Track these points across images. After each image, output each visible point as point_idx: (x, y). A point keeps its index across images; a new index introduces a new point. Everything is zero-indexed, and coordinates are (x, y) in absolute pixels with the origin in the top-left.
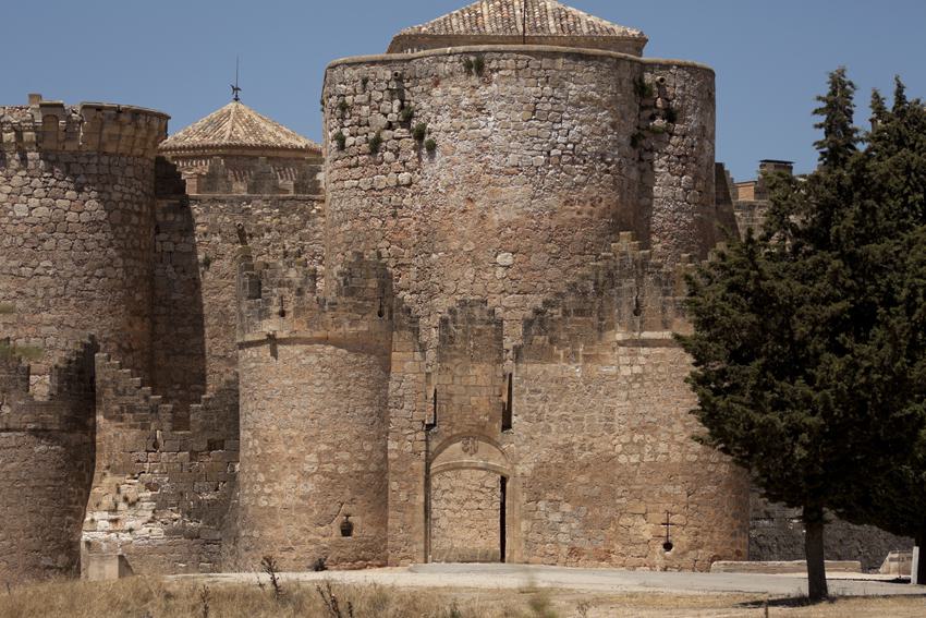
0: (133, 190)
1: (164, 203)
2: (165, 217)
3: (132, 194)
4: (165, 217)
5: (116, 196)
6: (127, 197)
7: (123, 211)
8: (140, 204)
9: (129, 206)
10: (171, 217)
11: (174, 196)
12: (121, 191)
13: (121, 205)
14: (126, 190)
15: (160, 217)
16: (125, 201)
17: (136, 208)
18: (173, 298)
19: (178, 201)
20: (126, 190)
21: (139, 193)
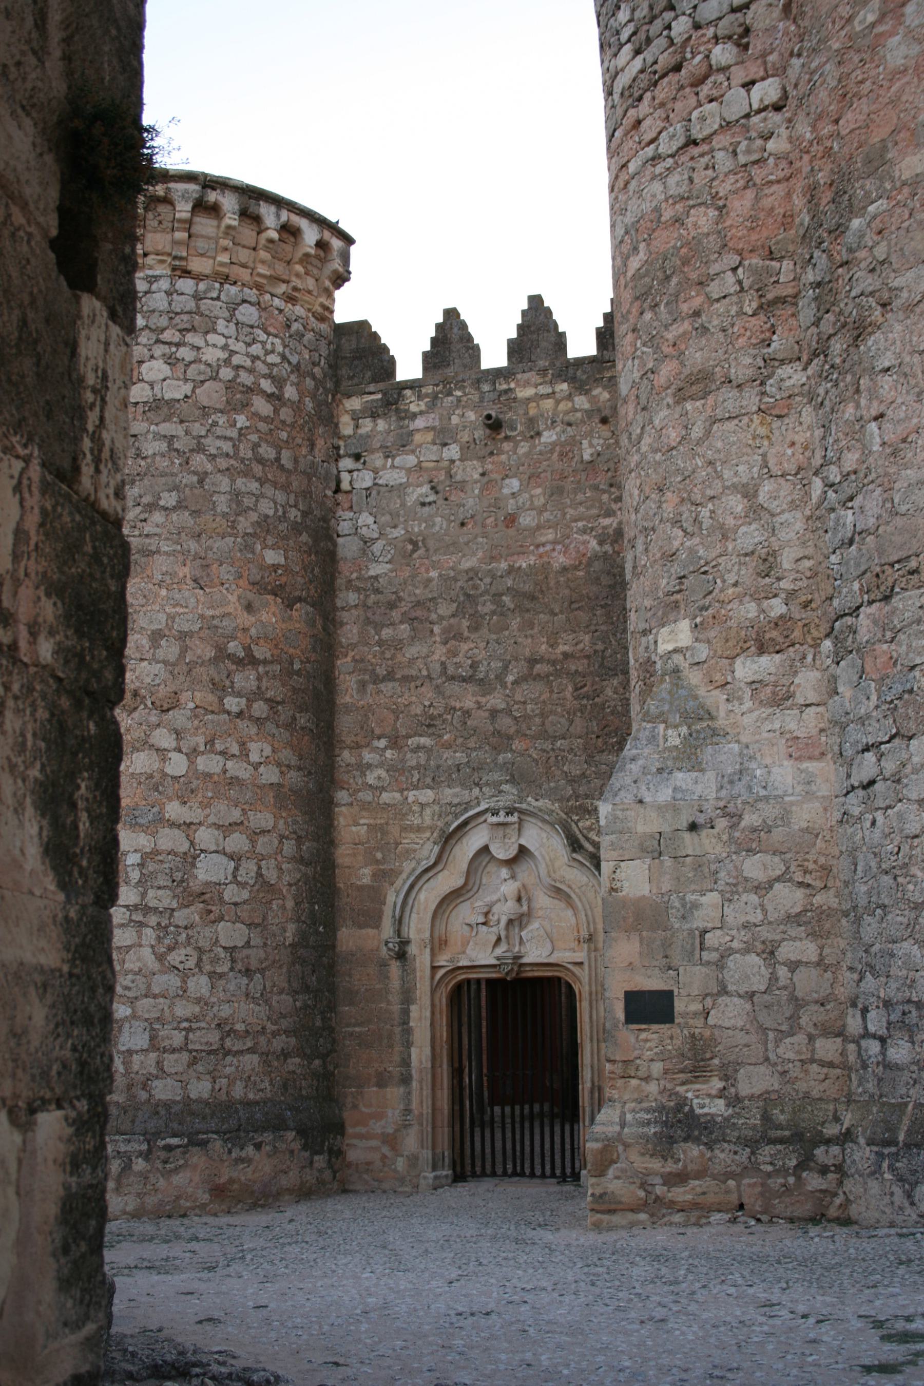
0: (256, 349)
1: (355, 403)
2: (357, 427)
3: (255, 358)
4: (357, 427)
5: (212, 355)
6: (236, 360)
7: (230, 385)
8: (279, 382)
9: (245, 378)
10: (367, 425)
11: (371, 388)
12: (225, 347)
13: (226, 373)
14: (239, 347)
15: (347, 429)
16: (238, 368)
17: (266, 385)
18: (372, 573)
19: (379, 396)
20: (239, 347)
21: (272, 359)
